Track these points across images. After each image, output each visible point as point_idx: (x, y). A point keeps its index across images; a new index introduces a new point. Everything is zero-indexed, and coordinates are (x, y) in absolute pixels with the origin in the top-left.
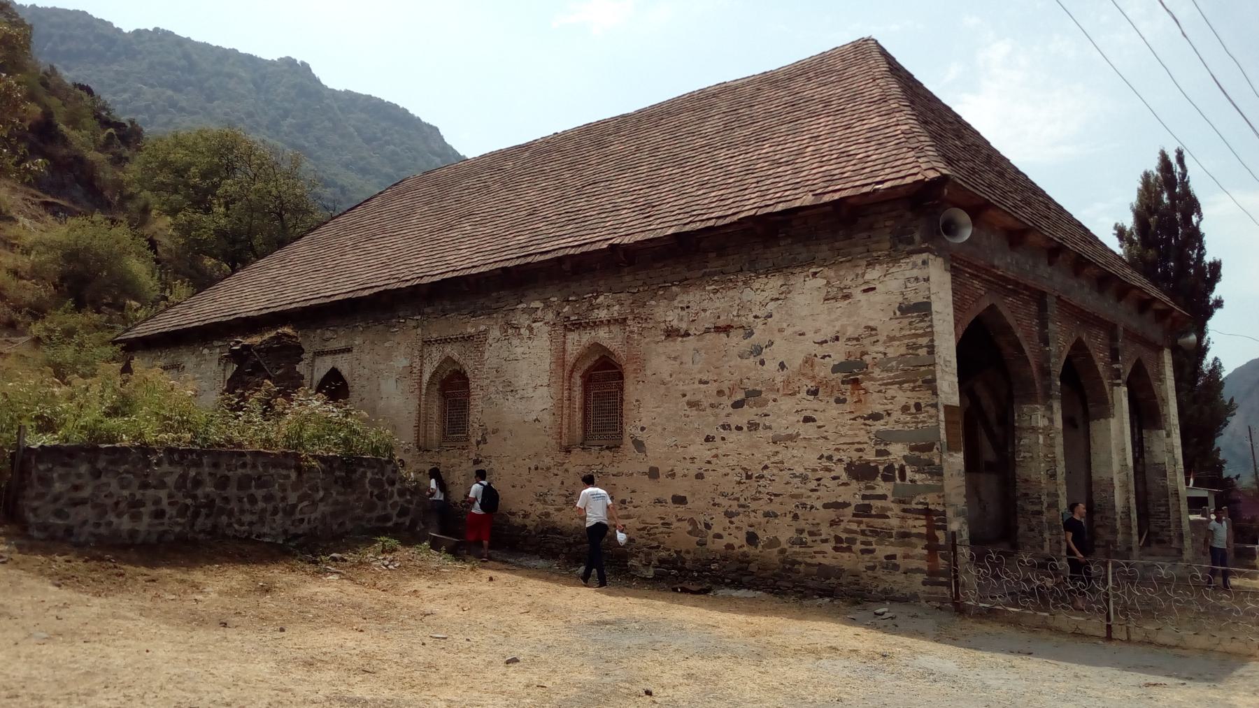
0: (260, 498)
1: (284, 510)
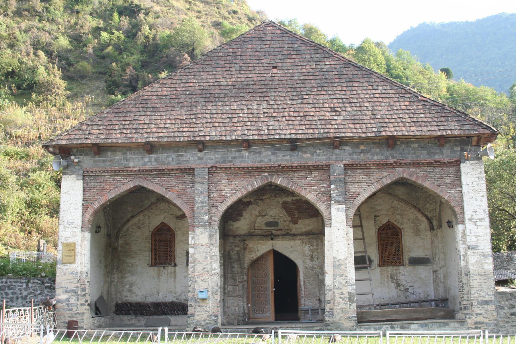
1: (21, 297)
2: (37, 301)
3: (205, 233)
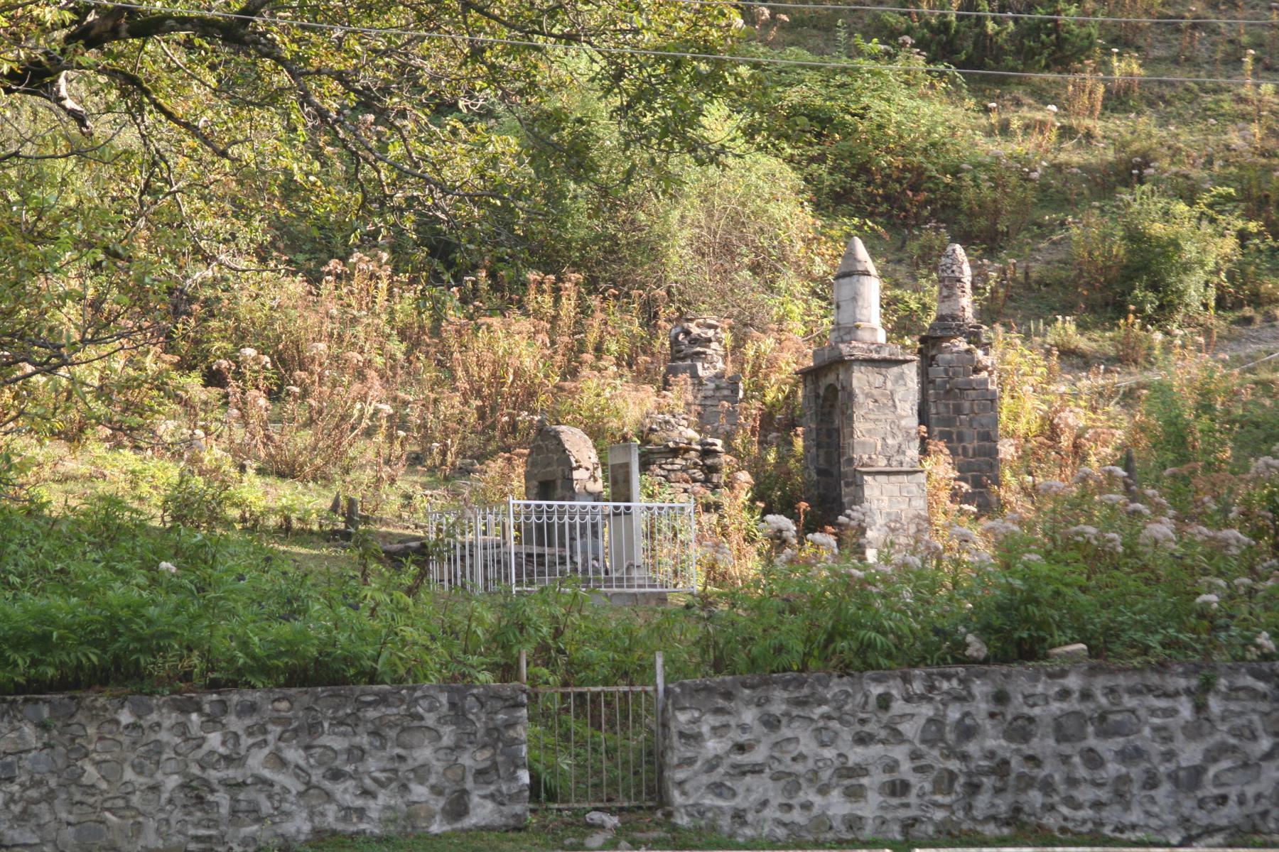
0: (1108, 756)
1: (1173, 777)
2: (1258, 797)
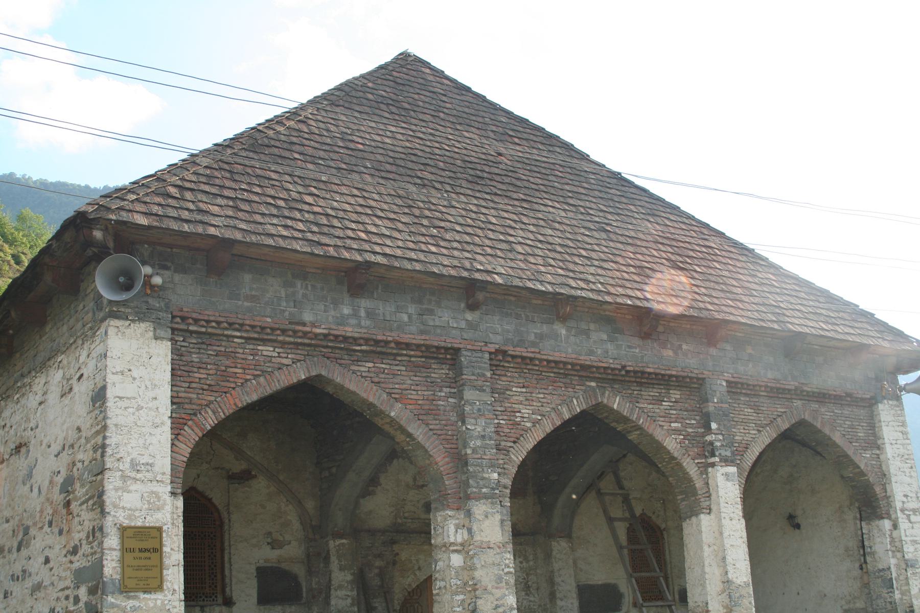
3: (493, 514)
